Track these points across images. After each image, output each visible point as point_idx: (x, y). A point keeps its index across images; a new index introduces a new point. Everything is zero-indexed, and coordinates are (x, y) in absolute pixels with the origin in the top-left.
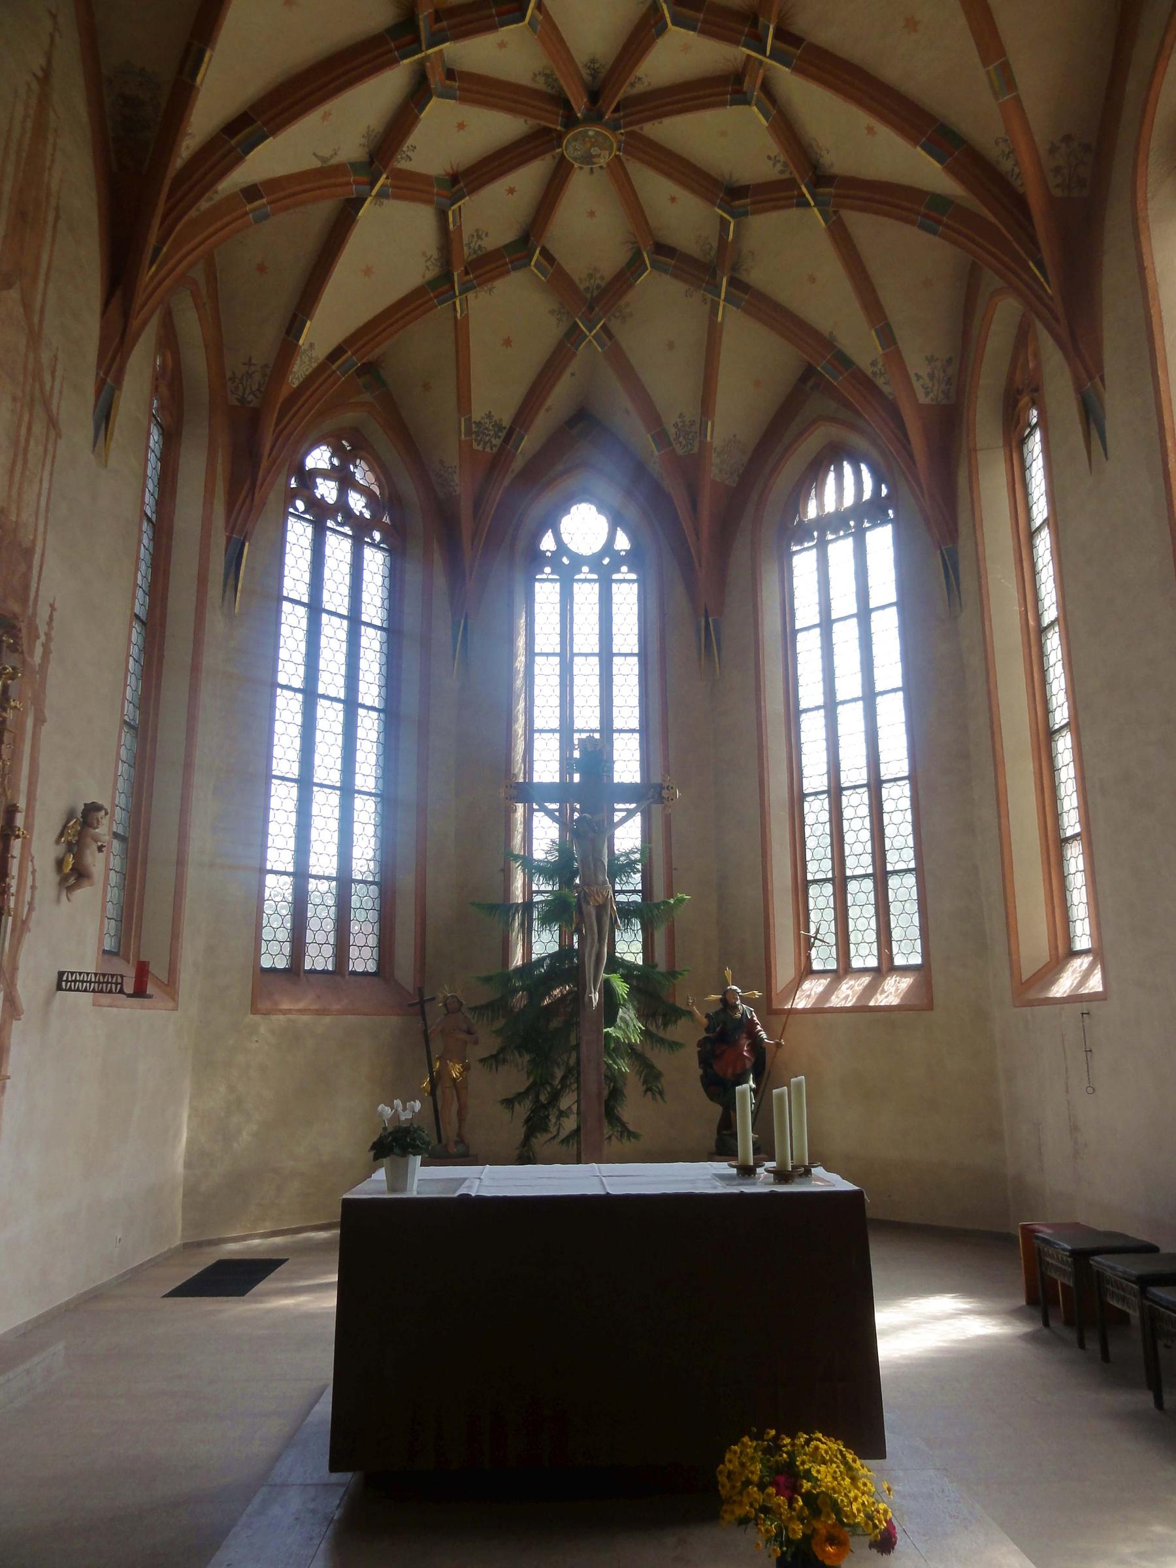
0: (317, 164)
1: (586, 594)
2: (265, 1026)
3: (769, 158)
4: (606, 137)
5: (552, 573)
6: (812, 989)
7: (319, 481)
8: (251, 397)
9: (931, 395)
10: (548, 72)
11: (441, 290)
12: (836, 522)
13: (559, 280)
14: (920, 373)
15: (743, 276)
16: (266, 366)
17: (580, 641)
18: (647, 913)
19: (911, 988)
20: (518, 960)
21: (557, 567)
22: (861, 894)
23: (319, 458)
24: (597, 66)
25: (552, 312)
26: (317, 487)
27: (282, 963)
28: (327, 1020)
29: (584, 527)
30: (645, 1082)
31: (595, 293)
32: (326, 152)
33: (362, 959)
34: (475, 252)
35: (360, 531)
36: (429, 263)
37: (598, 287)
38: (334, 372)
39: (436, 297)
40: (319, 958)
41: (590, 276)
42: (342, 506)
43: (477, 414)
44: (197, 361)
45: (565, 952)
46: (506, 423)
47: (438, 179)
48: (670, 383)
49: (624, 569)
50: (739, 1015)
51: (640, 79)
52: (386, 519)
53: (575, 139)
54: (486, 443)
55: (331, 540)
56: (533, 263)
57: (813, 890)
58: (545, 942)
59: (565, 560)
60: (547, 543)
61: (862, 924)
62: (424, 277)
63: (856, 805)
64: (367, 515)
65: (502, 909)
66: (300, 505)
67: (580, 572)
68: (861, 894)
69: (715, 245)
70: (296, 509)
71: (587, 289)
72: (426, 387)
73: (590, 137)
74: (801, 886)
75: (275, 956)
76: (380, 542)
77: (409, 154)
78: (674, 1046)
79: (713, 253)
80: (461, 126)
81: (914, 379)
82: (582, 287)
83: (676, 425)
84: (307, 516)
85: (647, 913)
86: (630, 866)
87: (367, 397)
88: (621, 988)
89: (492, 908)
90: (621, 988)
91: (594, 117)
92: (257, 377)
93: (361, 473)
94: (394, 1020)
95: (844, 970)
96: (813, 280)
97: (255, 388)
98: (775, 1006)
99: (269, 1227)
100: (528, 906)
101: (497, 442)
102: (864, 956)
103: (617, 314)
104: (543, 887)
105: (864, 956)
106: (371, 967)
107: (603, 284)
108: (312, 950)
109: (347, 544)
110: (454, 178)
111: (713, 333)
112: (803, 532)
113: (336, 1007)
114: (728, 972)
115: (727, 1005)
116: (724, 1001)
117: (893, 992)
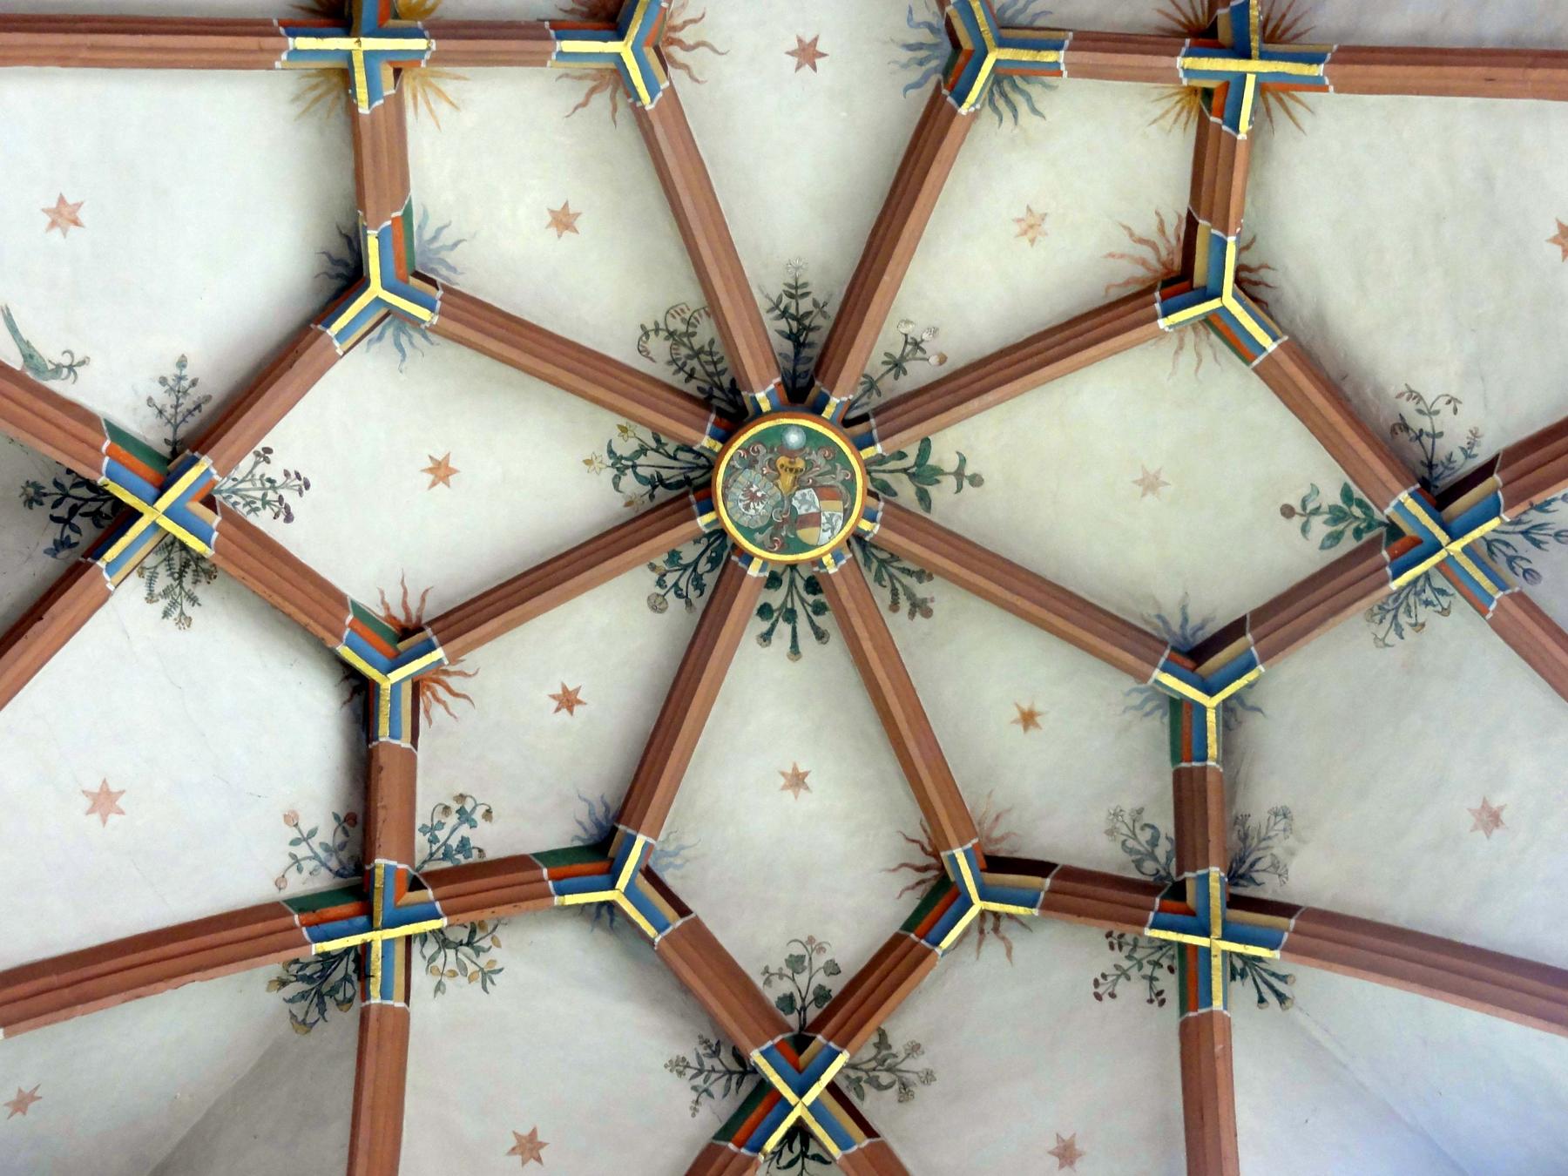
3: (1288, 512)
10: (677, 325)
15: (1269, 888)
24: (805, 305)
31: (813, 1013)
32: (51, 352)
34: (446, 856)
36: (302, 851)
37: (821, 995)
41: (796, 963)
51: (917, 345)
62: (280, 882)
69: (1167, 826)
71: (788, 1002)
73: (791, 454)
77: (290, 497)
79: (1164, 848)
82: (772, 995)
91: (800, 394)
96: (1491, 819)
103: (885, 1078)
107: (836, 986)
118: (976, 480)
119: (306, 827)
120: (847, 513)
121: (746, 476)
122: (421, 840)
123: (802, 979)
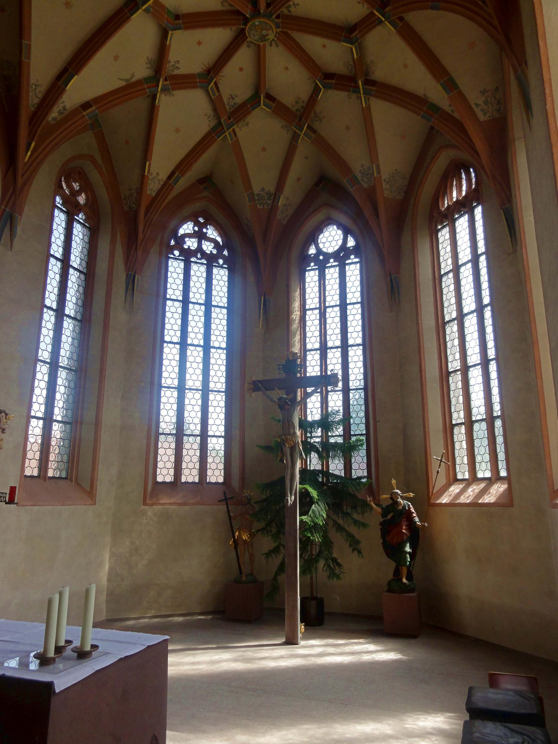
0: (123, 83)
1: (332, 274)
2: (150, 511)
4: (266, 23)
5: (314, 266)
6: (455, 489)
7: (187, 239)
8: (134, 205)
9: (488, 114)
11: (219, 130)
13: (279, 109)
14: (478, 102)
15: (372, 78)
16: (137, 189)
17: (332, 301)
19: (505, 491)
23: (187, 228)
25: (283, 127)
26: (185, 243)
27: (169, 479)
28: (187, 508)
29: (331, 239)
30: (350, 546)
31: (302, 111)
32: (128, 76)
33: (216, 475)
35: (211, 261)
36: (210, 119)
37: (303, 107)
38: (171, 184)
39: (216, 135)
40: (190, 475)
41: (297, 102)
42: (199, 249)
43: (256, 190)
44: (103, 193)
46: (272, 191)
47: (199, 75)
49: (352, 257)
50: (401, 507)
52: (226, 253)
53: (251, 29)
54: (264, 204)
55: (194, 267)
56: (262, 104)
57: (456, 430)
60: (312, 251)
61: (482, 450)
62: (209, 126)
64: (215, 252)
66: (177, 253)
67: (329, 262)
70: (174, 255)
71: (297, 110)
72: (232, 182)
73: (258, 26)
74: (449, 428)
76: (223, 264)
77: (177, 65)
78: (364, 525)
80: (199, 43)
81: (475, 108)
82: (294, 110)
83: (360, 172)
84: (181, 258)
87: (206, 194)
92: (135, 195)
93: (211, 232)
95: (474, 479)
96: (406, 66)
97: (134, 200)
98: (432, 501)
99: (152, 613)
101: (269, 202)
106: (221, 480)
107: (304, 105)
108: (185, 472)
109: (203, 269)
110: (209, 71)
113: (192, 501)
114: (394, 481)
116: (392, 498)
118: (298, 5)
119: (209, 115)
120: (273, 32)
121: (251, 33)
122: (227, 107)
123: (299, 105)
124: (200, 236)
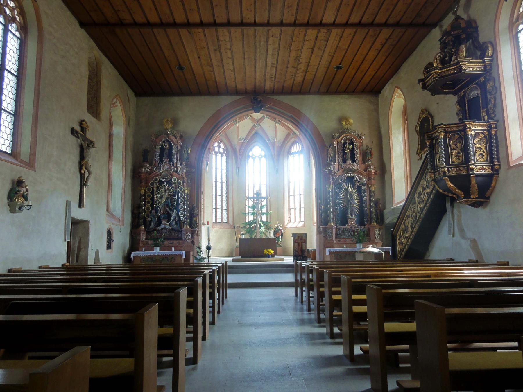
12: (296, 153)
18: (267, 214)
20: (247, 221)
21: (253, 158)
22: (298, 211)
23: (216, 144)
33: (225, 221)
35: (222, 154)
40: (219, 220)
42: (219, 152)
45: (254, 220)
48: (270, 133)
58: (251, 218)
59: (254, 157)
60: (251, 154)
63: (297, 197)
65: (246, 213)
66: (213, 152)
68: (298, 211)
74: (289, 210)
75: (214, 221)
85: (267, 214)
86: (264, 207)
88: (262, 224)
89: (244, 213)
90: (262, 224)
93: (222, 145)
94: (230, 230)
100: (248, 213)
102: (298, 219)
104: (251, 211)
105: (298, 219)
111: (276, 127)
112: (291, 154)
115: (278, 227)
117: (301, 224)
124: (219, 146)
